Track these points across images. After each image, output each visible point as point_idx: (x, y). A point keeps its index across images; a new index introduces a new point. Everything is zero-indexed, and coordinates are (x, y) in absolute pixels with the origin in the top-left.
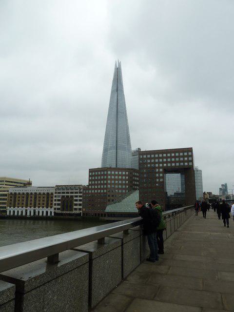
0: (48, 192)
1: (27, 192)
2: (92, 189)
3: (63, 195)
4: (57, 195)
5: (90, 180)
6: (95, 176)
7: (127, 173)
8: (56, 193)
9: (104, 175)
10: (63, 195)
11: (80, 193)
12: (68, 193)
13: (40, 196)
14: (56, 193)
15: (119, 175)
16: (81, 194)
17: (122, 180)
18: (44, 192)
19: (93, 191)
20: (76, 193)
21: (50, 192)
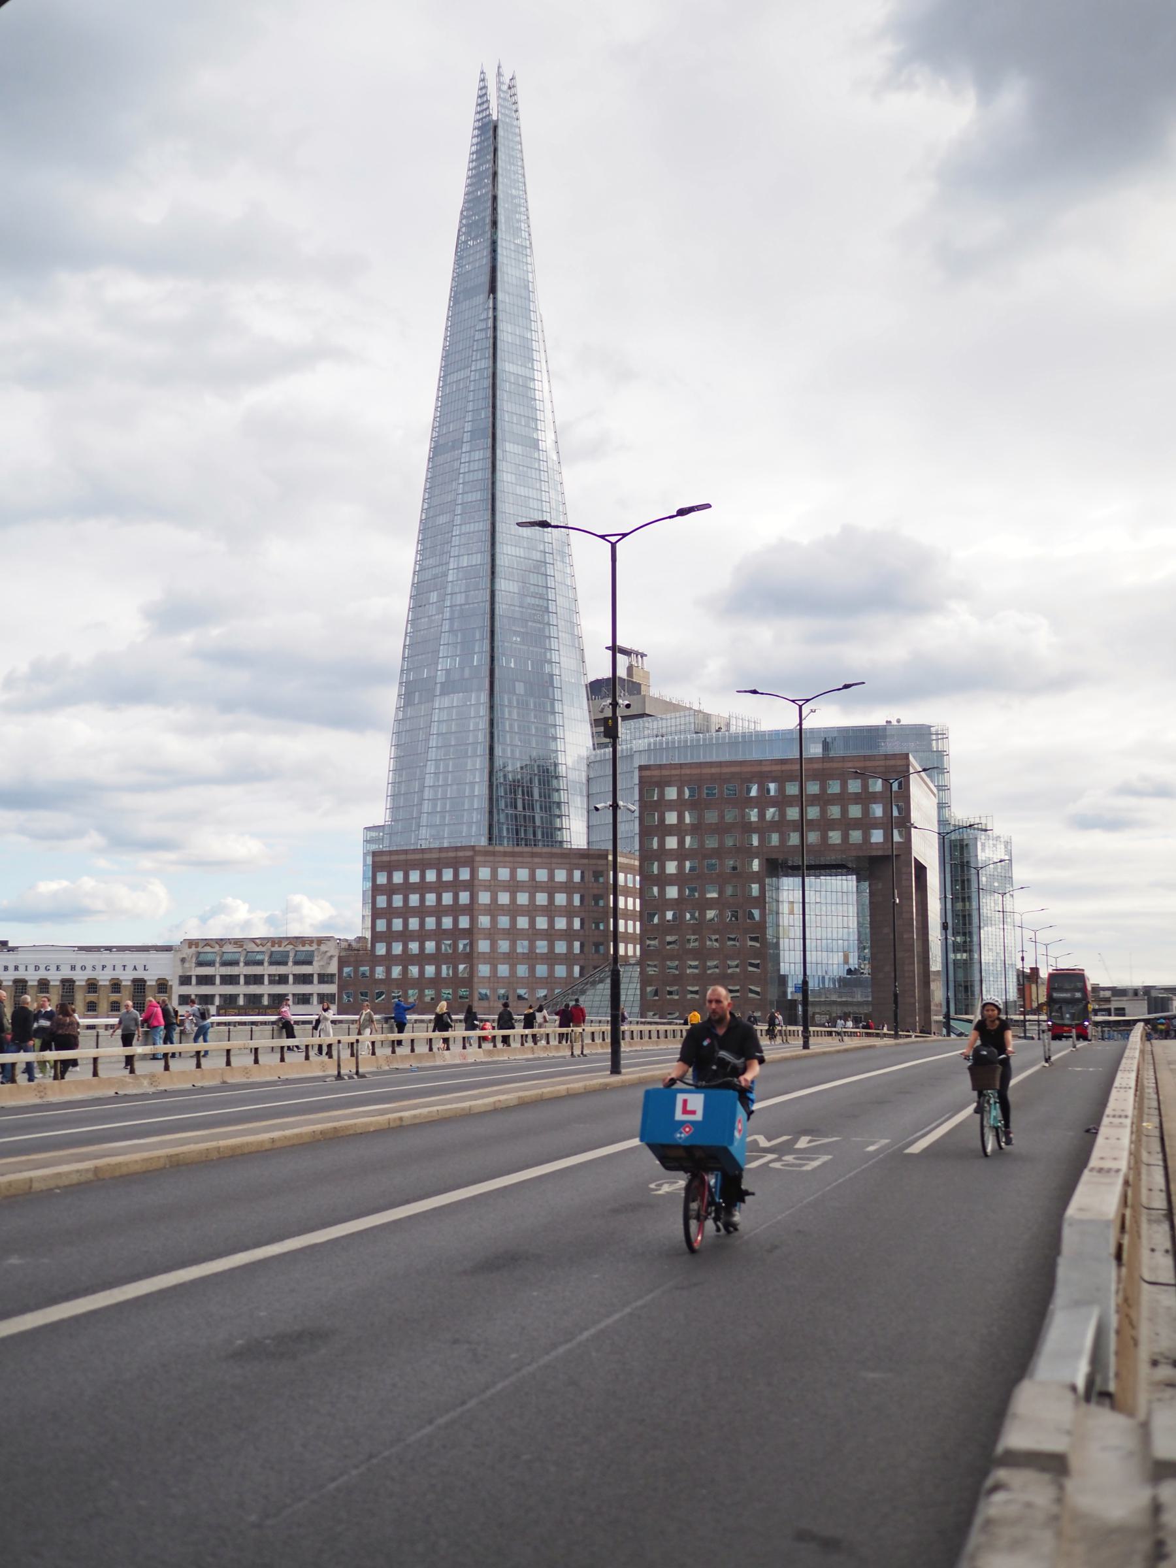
0: (140, 974)
1: (21, 974)
2: (389, 960)
3: (229, 990)
4: (193, 990)
5: (376, 914)
6: (406, 888)
7: (577, 875)
8: (185, 980)
9: (456, 886)
10: (229, 990)
11: (324, 979)
12: (257, 979)
13: (92, 997)
14: (185, 980)
15: (533, 887)
16: (332, 989)
17: (550, 911)
18: (120, 974)
19: (396, 972)
20: (305, 979)
21: (151, 978)
